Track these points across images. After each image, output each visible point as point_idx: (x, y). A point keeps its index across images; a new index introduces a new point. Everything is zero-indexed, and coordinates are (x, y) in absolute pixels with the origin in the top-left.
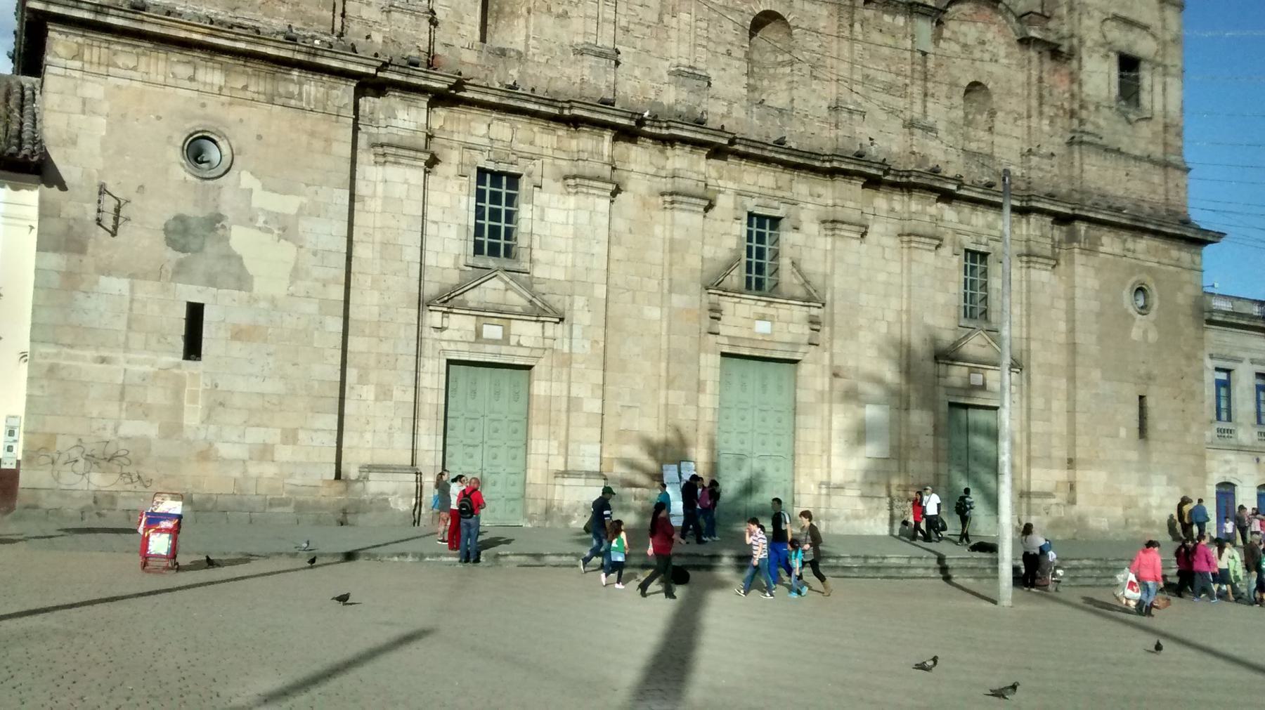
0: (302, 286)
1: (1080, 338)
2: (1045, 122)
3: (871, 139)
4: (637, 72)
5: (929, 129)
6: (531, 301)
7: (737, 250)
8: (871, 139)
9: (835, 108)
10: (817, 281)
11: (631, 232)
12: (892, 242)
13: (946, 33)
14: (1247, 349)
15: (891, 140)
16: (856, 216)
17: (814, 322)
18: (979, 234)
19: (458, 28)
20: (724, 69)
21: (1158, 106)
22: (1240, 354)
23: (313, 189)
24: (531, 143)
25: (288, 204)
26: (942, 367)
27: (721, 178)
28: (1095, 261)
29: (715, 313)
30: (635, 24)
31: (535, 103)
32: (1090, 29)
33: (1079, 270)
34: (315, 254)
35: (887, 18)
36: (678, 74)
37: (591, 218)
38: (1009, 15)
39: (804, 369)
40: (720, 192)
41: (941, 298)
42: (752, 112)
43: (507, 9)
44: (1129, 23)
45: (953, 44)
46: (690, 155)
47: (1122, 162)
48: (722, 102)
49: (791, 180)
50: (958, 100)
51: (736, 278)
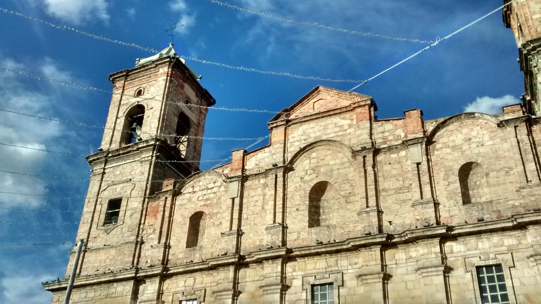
3: (390, 222)
4: (251, 236)
8: (390, 222)
15: (404, 217)
18: (487, 254)
19: (178, 246)
20: (295, 218)
30: (251, 215)
31: (198, 265)
38: (485, 116)
42: (311, 233)
46: (272, 265)
48: (293, 234)
49: (337, 261)
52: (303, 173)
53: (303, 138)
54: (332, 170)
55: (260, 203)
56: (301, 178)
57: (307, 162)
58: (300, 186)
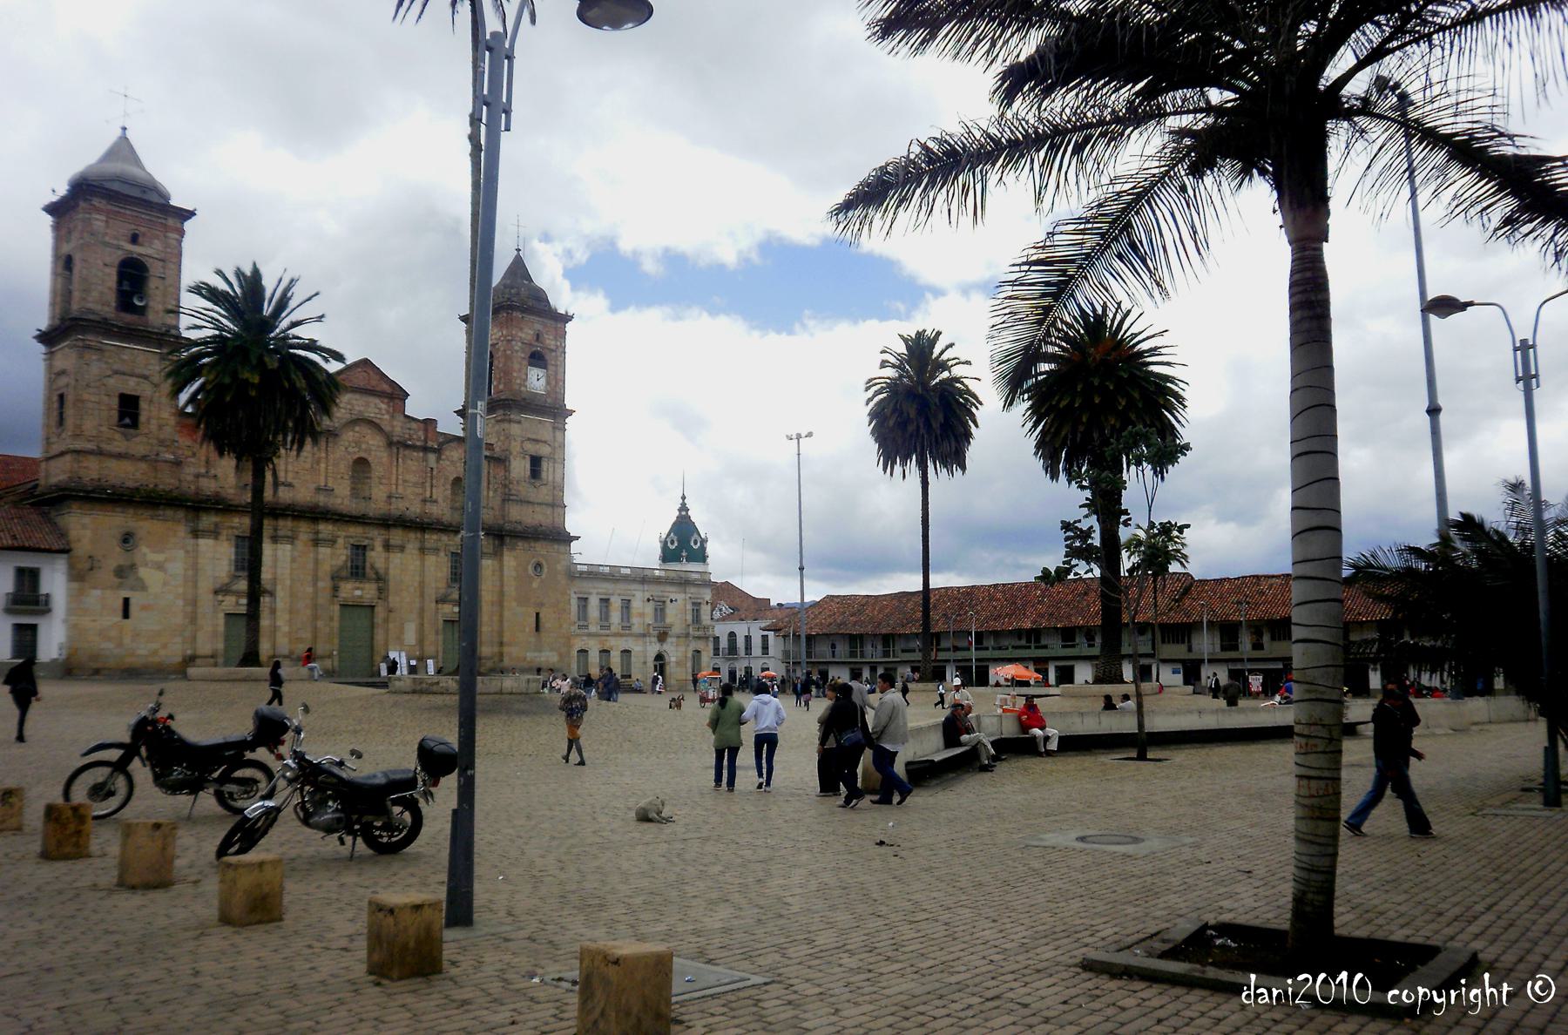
1: (506, 589)
2: (491, 494)
5: (436, 501)
7: (346, 561)
9: (390, 497)
10: (382, 572)
12: (416, 552)
13: (443, 457)
14: (595, 588)
16: (399, 542)
17: (380, 590)
21: (550, 478)
22: (591, 591)
25: (160, 557)
26: (440, 606)
28: (514, 553)
29: (335, 589)
32: (515, 447)
33: (506, 558)
35: (415, 454)
36: (318, 489)
39: (376, 609)
41: (439, 575)
44: (537, 441)
47: (530, 506)
50: (449, 487)
51: (344, 573)
52: (347, 444)
53: (349, 407)
54: (370, 450)
55: (309, 460)
57: (351, 433)
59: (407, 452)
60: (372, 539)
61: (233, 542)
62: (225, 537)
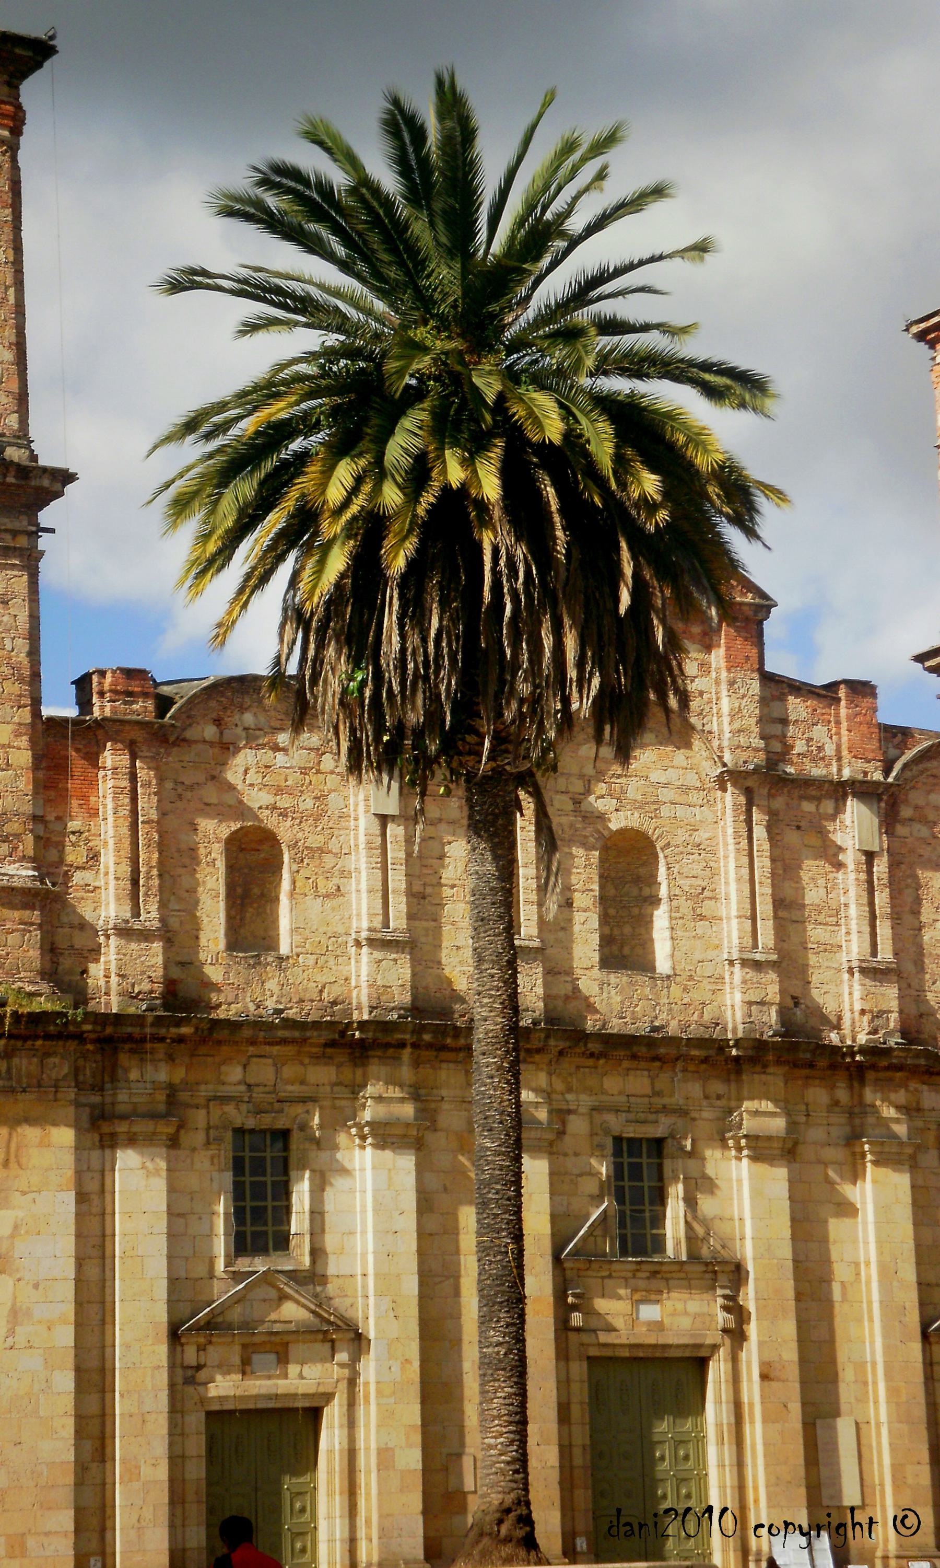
0: (22, 1332)
3: (793, 998)
6: (313, 1312)
8: (793, 998)
11: (445, 1189)
23: (29, 1197)
24: (303, 1083)
27: (570, 1090)
34: (36, 1286)
37: (390, 1178)
40: (570, 1112)
43: (256, 891)
45: (917, 826)
56: (577, 802)
58: (571, 825)
59: (779, 803)
60: (682, 1112)
61: (226, 1151)
62: (201, 1137)
